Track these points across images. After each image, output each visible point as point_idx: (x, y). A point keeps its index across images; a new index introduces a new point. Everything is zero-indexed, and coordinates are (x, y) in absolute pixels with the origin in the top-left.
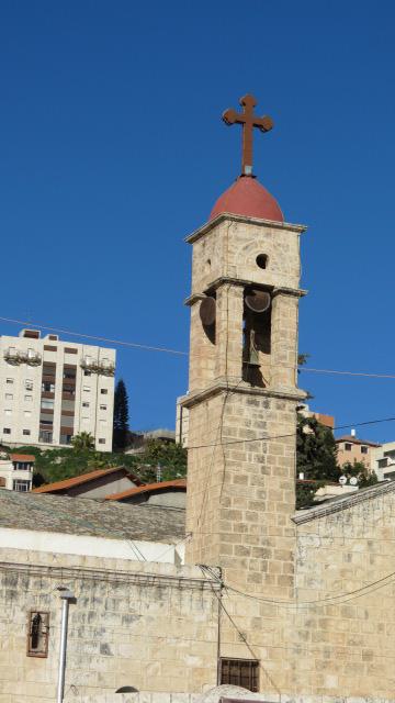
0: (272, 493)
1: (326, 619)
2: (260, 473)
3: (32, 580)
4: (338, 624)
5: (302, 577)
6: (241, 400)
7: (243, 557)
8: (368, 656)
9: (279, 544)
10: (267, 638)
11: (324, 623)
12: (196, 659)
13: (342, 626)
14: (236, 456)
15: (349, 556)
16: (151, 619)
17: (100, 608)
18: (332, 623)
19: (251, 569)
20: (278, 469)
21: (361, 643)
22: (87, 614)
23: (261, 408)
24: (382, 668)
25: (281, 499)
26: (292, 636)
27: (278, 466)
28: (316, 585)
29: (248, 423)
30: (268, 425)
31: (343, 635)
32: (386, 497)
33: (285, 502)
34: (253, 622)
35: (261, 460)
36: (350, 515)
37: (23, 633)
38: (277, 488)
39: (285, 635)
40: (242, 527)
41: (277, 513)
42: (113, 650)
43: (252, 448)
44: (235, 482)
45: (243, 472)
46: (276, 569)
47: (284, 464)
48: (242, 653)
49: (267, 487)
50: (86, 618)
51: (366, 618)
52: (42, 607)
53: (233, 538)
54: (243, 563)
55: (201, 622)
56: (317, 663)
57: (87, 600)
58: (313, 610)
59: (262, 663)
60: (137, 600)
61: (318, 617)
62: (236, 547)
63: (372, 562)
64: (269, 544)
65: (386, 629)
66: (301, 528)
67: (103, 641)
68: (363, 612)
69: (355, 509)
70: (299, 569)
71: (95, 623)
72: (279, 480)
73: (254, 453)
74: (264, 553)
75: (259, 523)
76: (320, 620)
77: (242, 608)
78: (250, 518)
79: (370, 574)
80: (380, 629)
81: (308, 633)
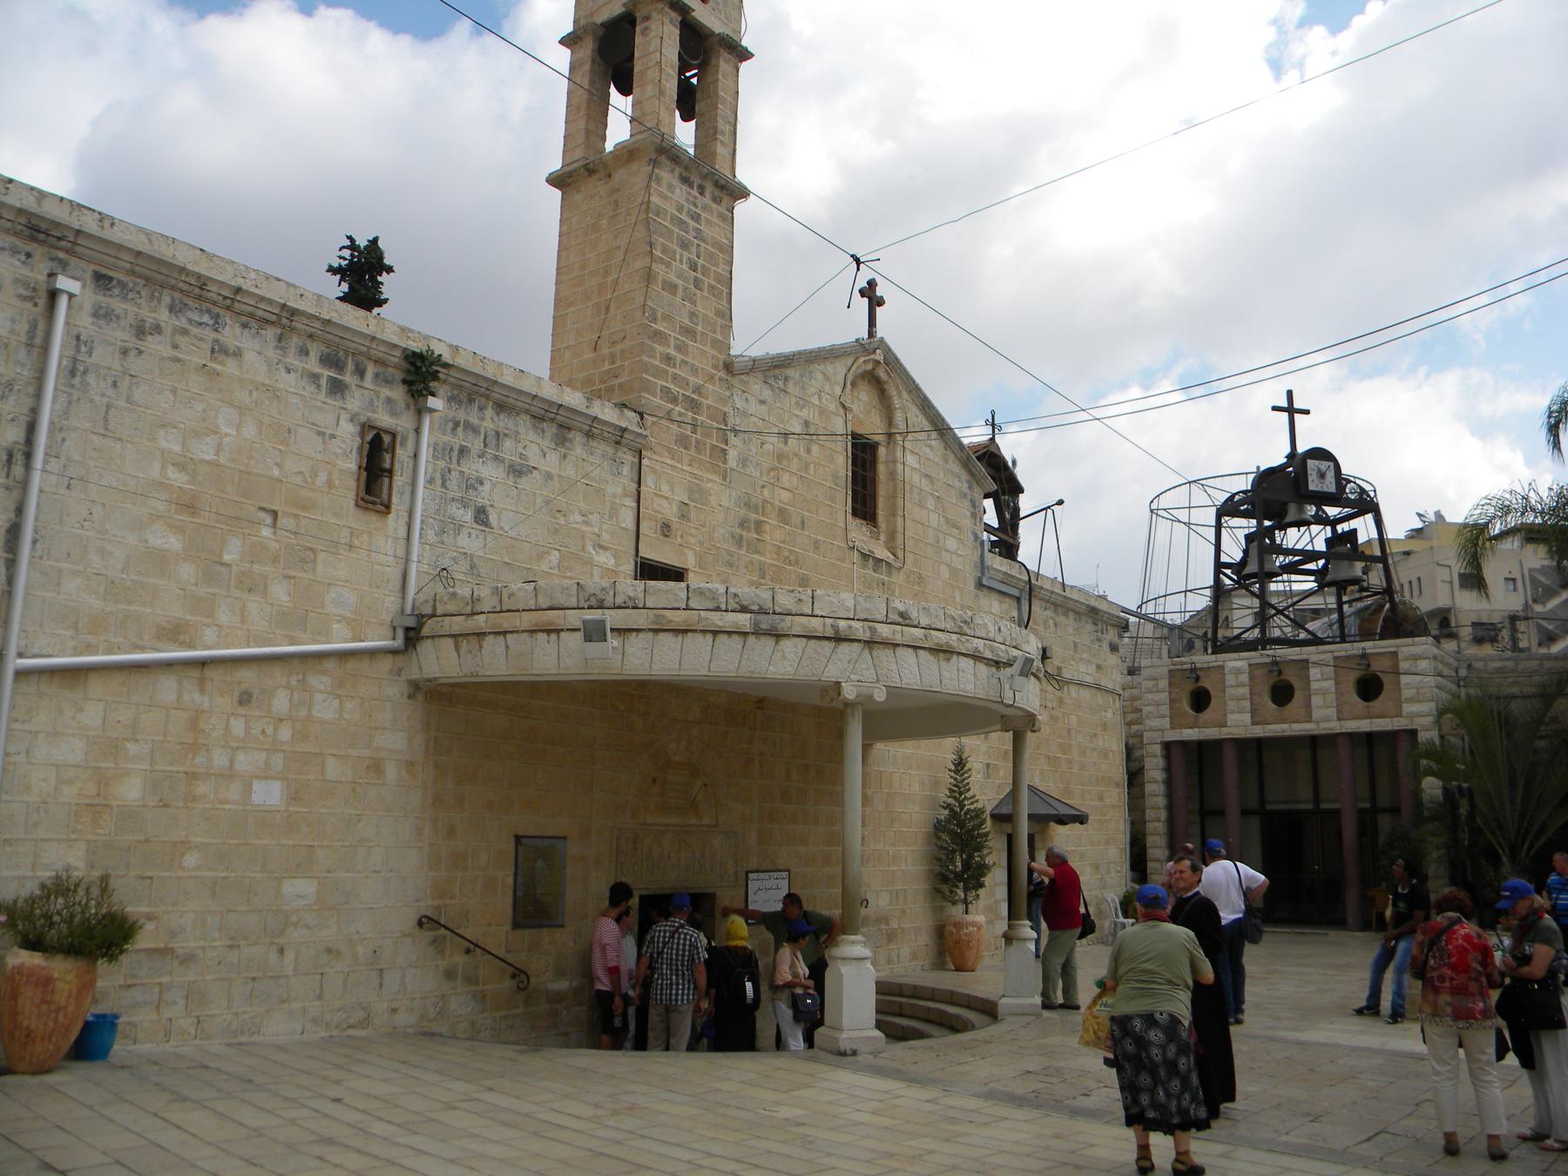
1: (762, 521)
3: (371, 370)
4: (774, 533)
6: (672, 171)
11: (759, 526)
12: (608, 554)
16: (549, 476)
17: (476, 444)
22: (456, 448)
23: (695, 192)
35: (694, 267)
37: (350, 464)
40: (668, 359)
42: (493, 518)
43: (684, 245)
45: (673, 278)
47: (719, 282)
50: (455, 454)
52: (384, 420)
55: (614, 495)
57: (457, 424)
58: (748, 505)
60: (533, 445)
61: (753, 516)
62: (662, 386)
64: (700, 394)
67: (481, 501)
71: (473, 467)
74: (694, 406)
78: (679, 349)
80: (817, 548)
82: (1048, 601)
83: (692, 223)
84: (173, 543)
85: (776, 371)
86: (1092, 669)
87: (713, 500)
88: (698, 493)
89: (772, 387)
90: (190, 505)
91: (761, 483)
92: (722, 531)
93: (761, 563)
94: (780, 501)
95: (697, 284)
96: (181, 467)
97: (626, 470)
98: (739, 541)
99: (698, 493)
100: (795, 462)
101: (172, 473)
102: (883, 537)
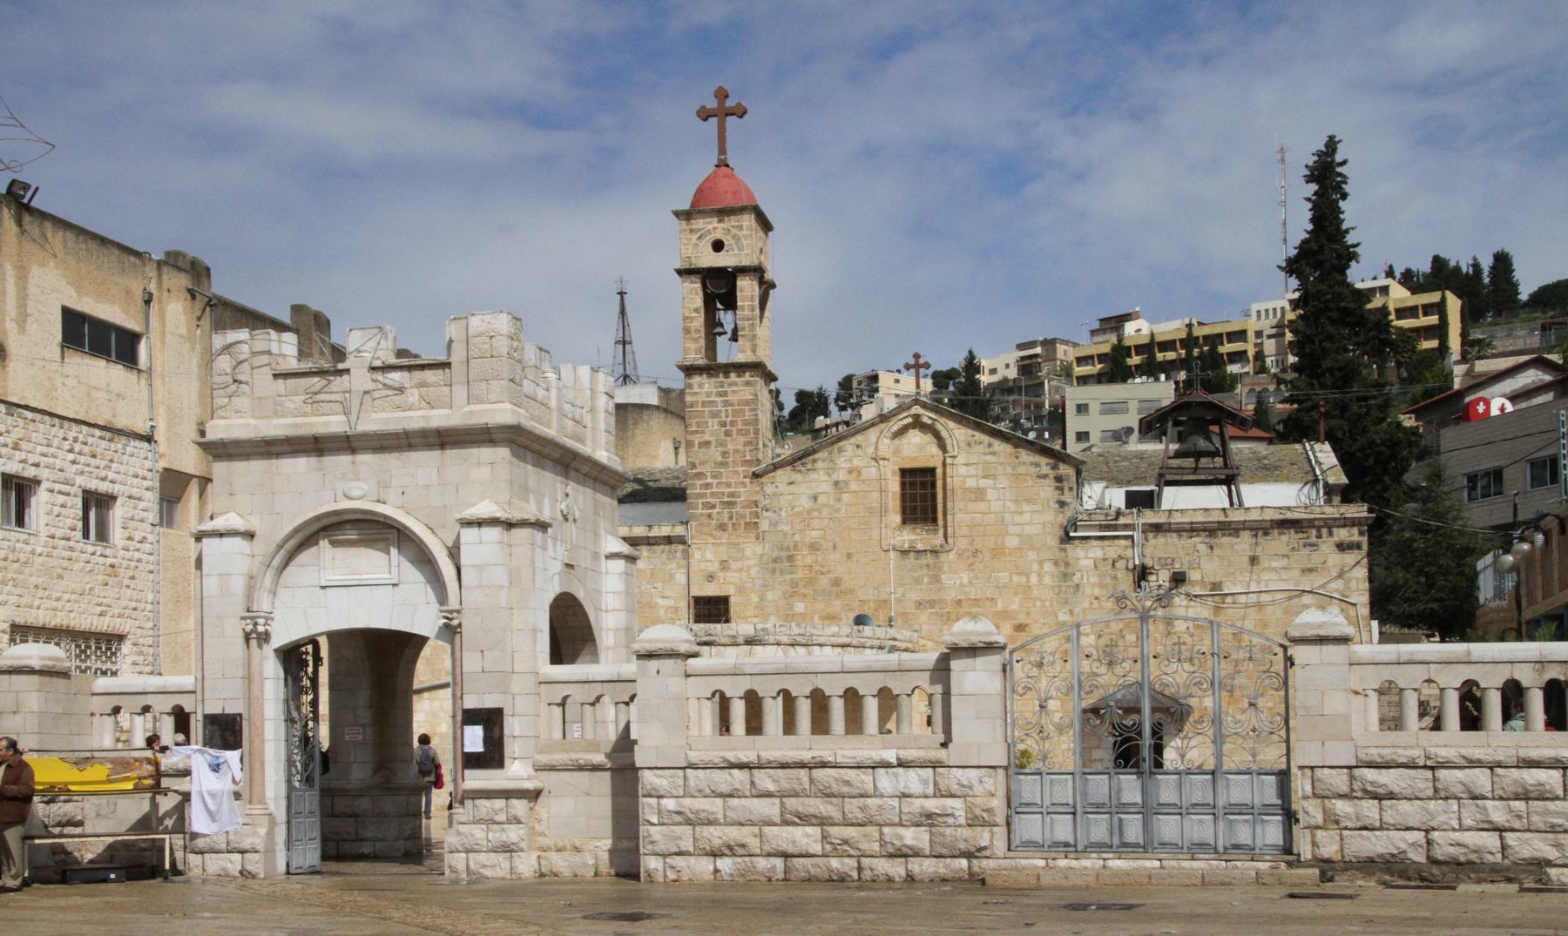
0: (736, 451)
2: (723, 438)
4: (805, 558)
5: (767, 521)
7: (710, 511)
8: (836, 582)
10: (733, 577)
11: (790, 558)
13: (809, 560)
14: (698, 424)
15: (815, 498)
18: (799, 557)
20: (741, 430)
21: (829, 572)
24: (852, 591)
25: (745, 456)
27: (740, 427)
28: (781, 527)
29: (709, 394)
30: (729, 393)
31: (811, 567)
32: (853, 440)
33: (748, 458)
35: (723, 424)
36: (814, 461)
38: (741, 447)
40: (707, 486)
41: (741, 469)
43: (715, 415)
44: (699, 448)
45: (707, 438)
46: (743, 516)
48: (711, 590)
49: (730, 447)
53: (699, 496)
54: (709, 516)
56: (784, 593)
59: (732, 600)
64: (734, 496)
65: (855, 558)
66: (763, 480)
68: (831, 544)
69: (819, 455)
70: (765, 514)
72: (742, 439)
73: (716, 420)
74: (730, 504)
75: (724, 480)
77: (705, 555)
78: (714, 477)
79: (838, 510)
82: (1192, 530)
83: (719, 399)
85: (803, 461)
86: (1296, 573)
89: (800, 471)
93: (792, 579)
95: (727, 434)
97: (678, 555)
98: (773, 571)
100: (825, 512)
102: (941, 532)
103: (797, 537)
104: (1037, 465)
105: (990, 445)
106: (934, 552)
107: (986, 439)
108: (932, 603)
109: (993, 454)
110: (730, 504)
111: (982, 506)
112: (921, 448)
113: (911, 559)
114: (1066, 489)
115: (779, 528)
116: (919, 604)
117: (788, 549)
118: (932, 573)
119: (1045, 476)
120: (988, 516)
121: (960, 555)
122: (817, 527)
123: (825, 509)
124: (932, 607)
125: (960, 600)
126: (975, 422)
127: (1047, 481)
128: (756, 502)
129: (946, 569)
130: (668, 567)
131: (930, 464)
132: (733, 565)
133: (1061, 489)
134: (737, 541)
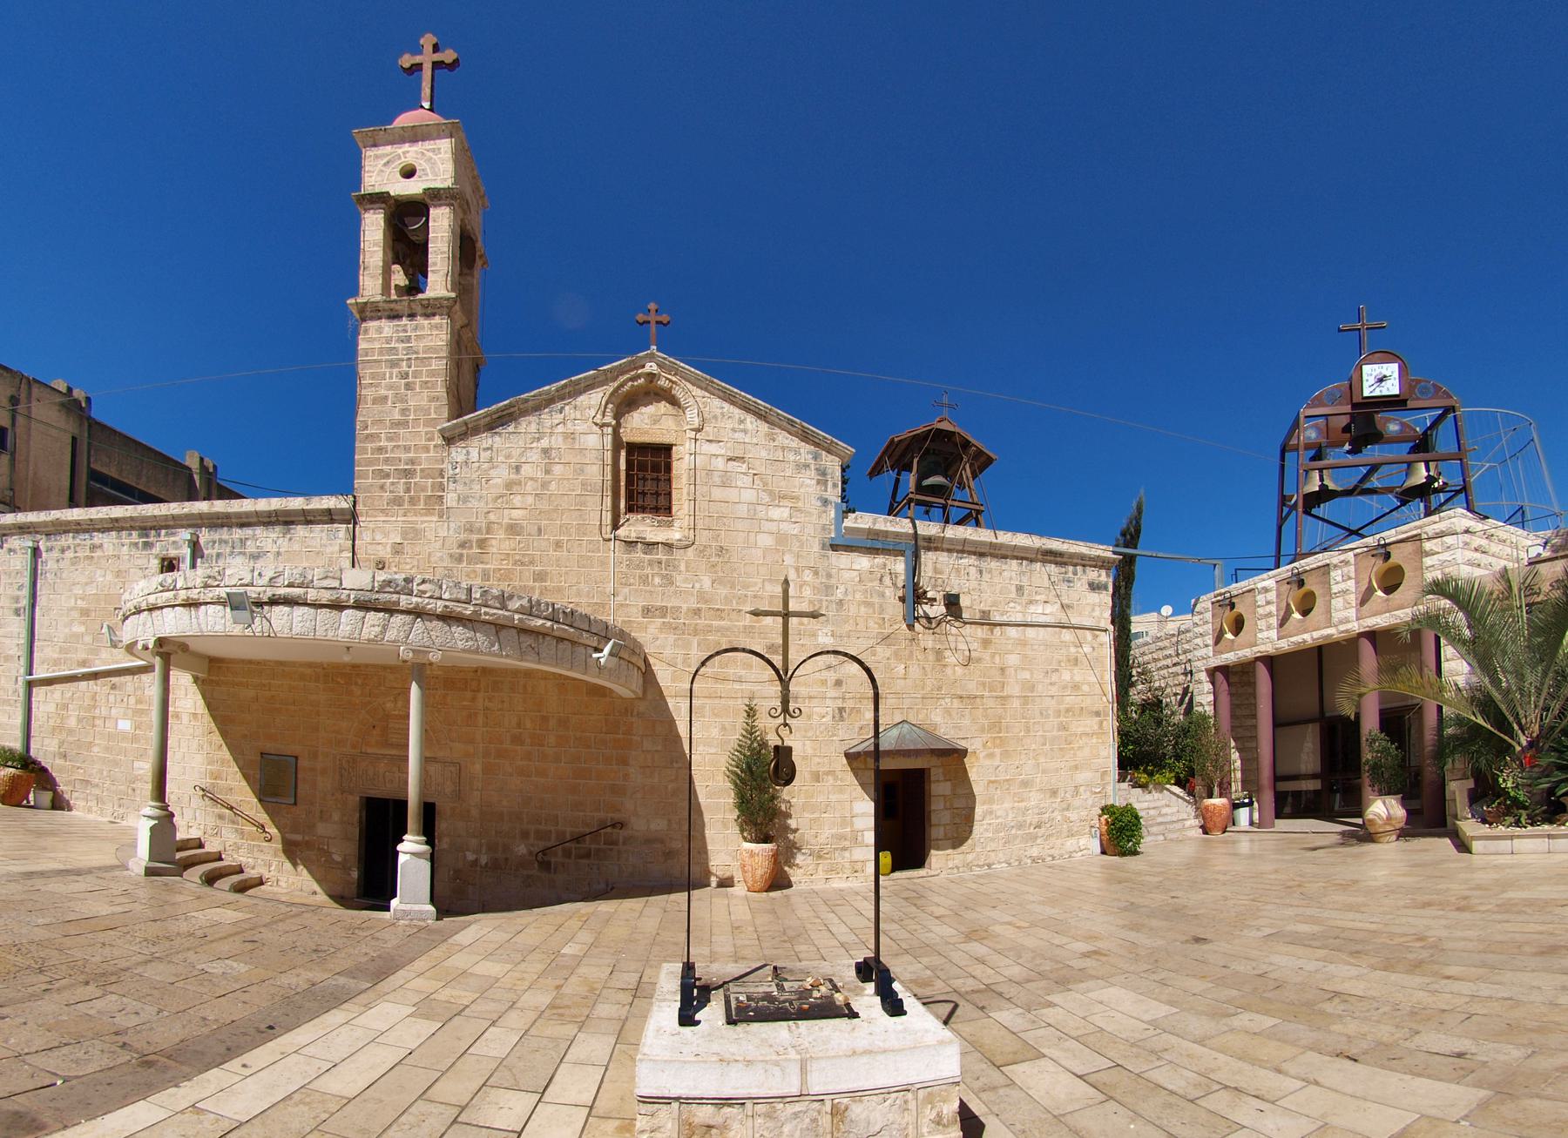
9: (426, 460)
11: (482, 543)
13: (507, 546)
18: (494, 542)
19: (390, 492)
21: (531, 563)
26: (441, 559)
28: (474, 503)
34: (393, 547)
39: (432, 559)
46: (424, 489)
51: (540, 534)
54: (382, 487)
61: (475, 537)
63: (547, 472)
70: (452, 486)
74: (408, 473)
76: (478, 541)
79: (545, 485)
81: (461, 555)
84: (82, 629)
87: (430, 535)
88: (412, 534)
90: (85, 613)
91: (486, 510)
92: (439, 554)
94: (511, 519)
96: (83, 599)
97: (342, 534)
99: (412, 534)
101: (79, 602)
103: (492, 517)
104: (797, 452)
105: (741, 421)
106: (669, 546)
107: (737, 412)
108: (663, 611)
109: (745, 431)
110: (408, 473)
111: (731, 494)
112: (656, 420)
113: (639, 554)
114: (830, 484)
115: (470, 505)
116: (647, 611)
117: (479, 531)
118: (664, 572)
119: (807, 466)
120: (737, 506)
121: (702, 552)
122: (519, 505)
123: (530, 483)
124: (664, 616)
125: (699, 610)
126: (724, 391)
127: (808, 472)
128: (442, 470)
129: (683, 568)
130: (329, 549)
131: (666, 440)
132: (407, 549)
133: (822, 482)
134: (414, 519)
